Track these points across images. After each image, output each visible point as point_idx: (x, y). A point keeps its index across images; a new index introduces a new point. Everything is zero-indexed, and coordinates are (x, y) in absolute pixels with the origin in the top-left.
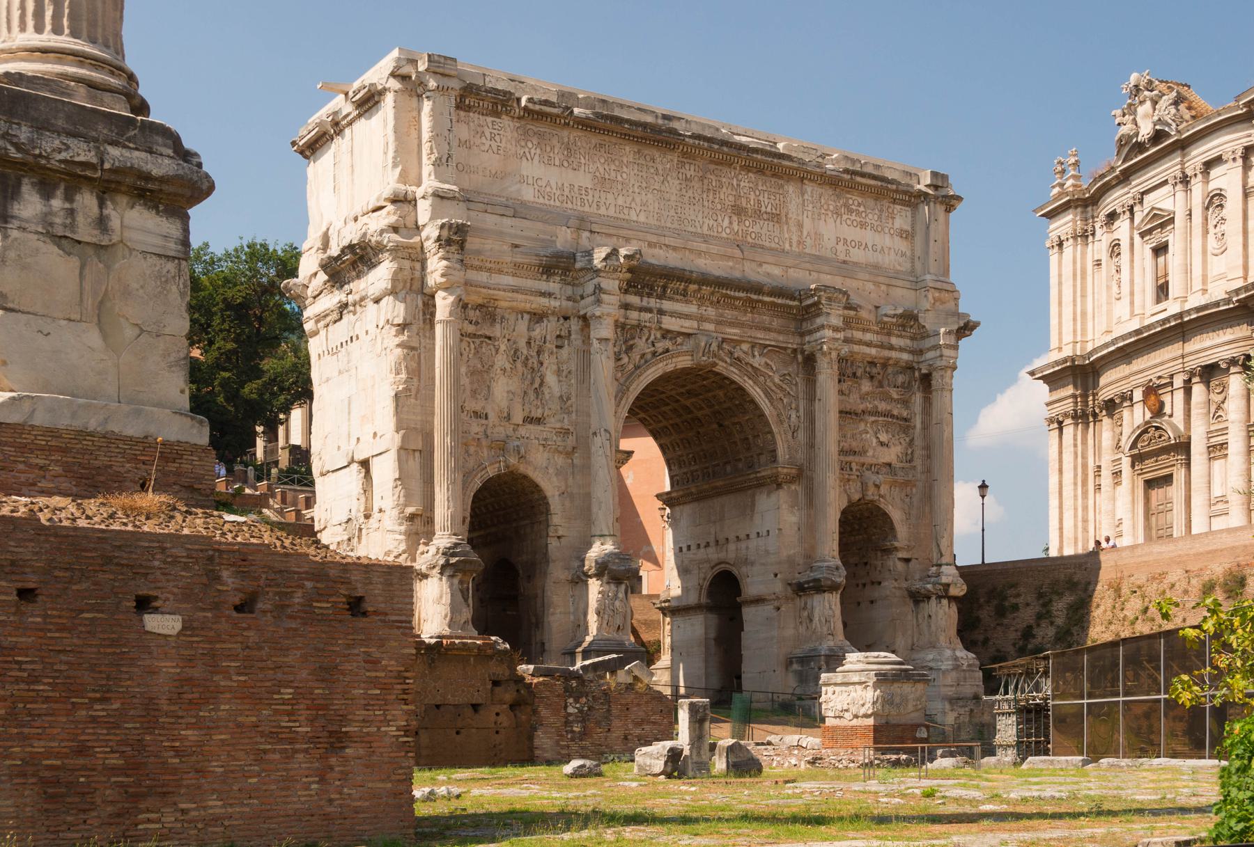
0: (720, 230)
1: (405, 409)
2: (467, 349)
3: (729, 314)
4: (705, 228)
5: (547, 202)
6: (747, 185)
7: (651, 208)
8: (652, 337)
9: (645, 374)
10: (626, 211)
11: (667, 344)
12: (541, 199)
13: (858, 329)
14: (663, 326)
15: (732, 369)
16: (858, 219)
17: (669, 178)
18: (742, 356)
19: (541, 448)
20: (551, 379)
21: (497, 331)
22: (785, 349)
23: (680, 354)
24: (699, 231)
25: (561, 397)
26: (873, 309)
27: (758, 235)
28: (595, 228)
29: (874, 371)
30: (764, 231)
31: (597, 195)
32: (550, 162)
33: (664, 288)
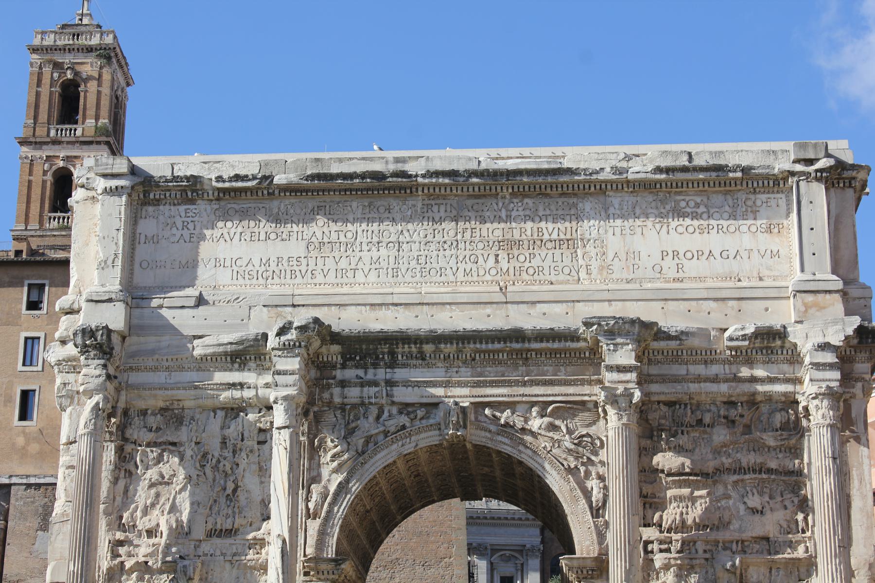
0: (482, 273)
1: (60, 537)
4: (461, 273)
6: (521, 213)
7: (384, 264)
8: (386, 414)
9: (372, 461)
11: (404, 420)
13: (695, 363)
14: (395, 399)
15: (500, 438)
16: (696, 223)
19: (228, 565)
21: (183, 435)
22: (583, 403)
23: (419, 431)
24: (452, 278)
25: (263, 501)
27: (539, 270)
29: (733, 413)
30: (546, 265)
31: (312, 263)
33: (392, 354)
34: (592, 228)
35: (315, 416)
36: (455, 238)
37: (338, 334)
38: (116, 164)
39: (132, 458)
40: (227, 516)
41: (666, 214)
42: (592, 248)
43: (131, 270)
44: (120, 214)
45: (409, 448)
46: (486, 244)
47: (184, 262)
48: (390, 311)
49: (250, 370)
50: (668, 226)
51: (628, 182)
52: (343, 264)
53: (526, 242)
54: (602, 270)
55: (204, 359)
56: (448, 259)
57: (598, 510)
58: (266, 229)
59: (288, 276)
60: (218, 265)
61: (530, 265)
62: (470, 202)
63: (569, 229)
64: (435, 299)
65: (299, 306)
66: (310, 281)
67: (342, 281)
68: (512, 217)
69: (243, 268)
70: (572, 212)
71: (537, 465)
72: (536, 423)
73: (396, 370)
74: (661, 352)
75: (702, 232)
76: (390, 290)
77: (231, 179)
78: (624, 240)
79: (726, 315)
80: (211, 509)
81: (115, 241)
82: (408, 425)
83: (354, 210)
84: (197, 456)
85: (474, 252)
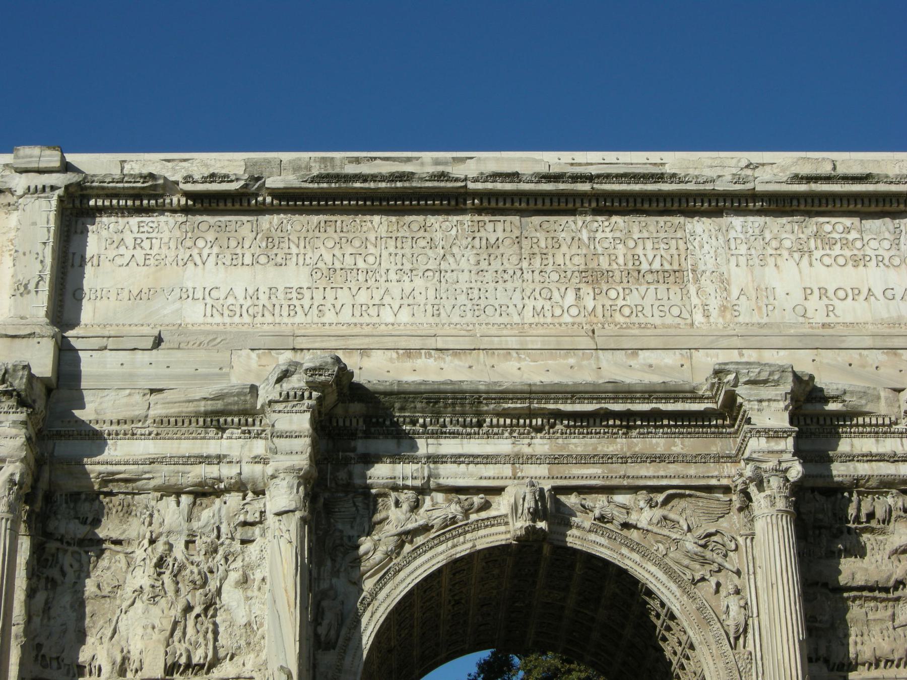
0: (558, 312)
2: (76, 566)
3: (579, 444)
4: (528, 313)
5: (227, 320)
6: (610, 235)
7: (421, 299)
10: (373, 311)
11: (454, 509)
12: (218, 319)
13: (862, 434)
14: (443, 481)
15: (592, 537)
16: (847, 253)
17: (455, 250)
18: (609, 511)
20: (231, 596)
23: (478, 526)
24: (516, 319)
25: (248, 624)
26: (891, 394)
27: (638, 310)
28: (301, 343)
30: (647, 302)
31: (318, 295)
32: (235, 261)
34: (708, 256)
35: (325, 504)
36: (519, 266)
37: (359, 386)
38: (44, 156)
39: (57, 562)
40: (197, 645)
41: (806, 240)
42: (709, 282)
43: (61, 301)
44: (48, 222)
45: (462, 548)
46: (563, 275)
47: (135, 292)
48: (432, 360)
49: (231, 438)
50: (810, 256)
51: (754, 196)
52: (363, 297)
53: (618, 274)
54: (724, 311)
55: (165, 420)
56: (510, 293)
57: (737, 638)
58: (252, 250)
59: (285, 313)
60: (184, 296)
61: (624, 303)
62: (536, 220)
63: (676, 257)
64: (496, 342)
65: (302, 350)
66: (316, 320)
67: (361, 320)
68: (597, 240)
69: (221, 301)
70: (679, 235)
71: (647, 575)
72: (644, 517)
73: (442, 441)
74: (815, 420)
75: (854, 264)
76: (432, 332)
77: (205, 180)
78: (752, 272)
79: (901, 371)
80: (172, 635)
81: (41, 258)
82: (460, 517)
83: (376, 227)
84: (151, 560)
85: (546, 285)
